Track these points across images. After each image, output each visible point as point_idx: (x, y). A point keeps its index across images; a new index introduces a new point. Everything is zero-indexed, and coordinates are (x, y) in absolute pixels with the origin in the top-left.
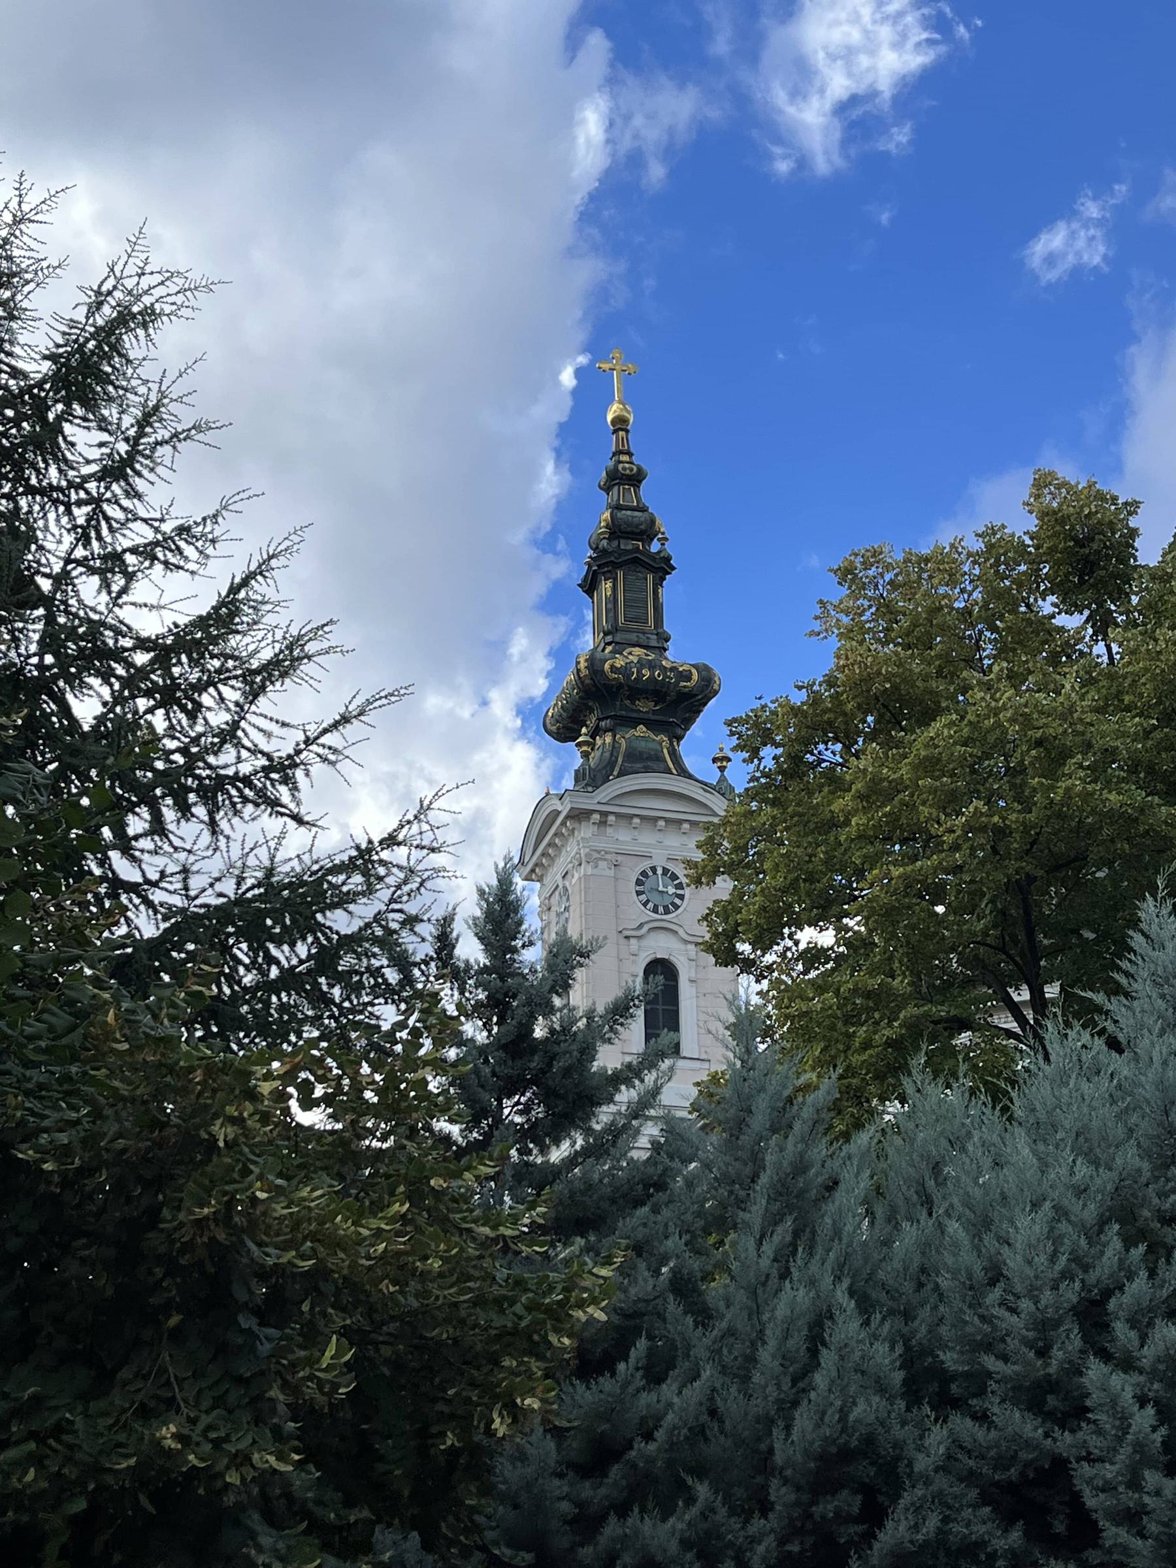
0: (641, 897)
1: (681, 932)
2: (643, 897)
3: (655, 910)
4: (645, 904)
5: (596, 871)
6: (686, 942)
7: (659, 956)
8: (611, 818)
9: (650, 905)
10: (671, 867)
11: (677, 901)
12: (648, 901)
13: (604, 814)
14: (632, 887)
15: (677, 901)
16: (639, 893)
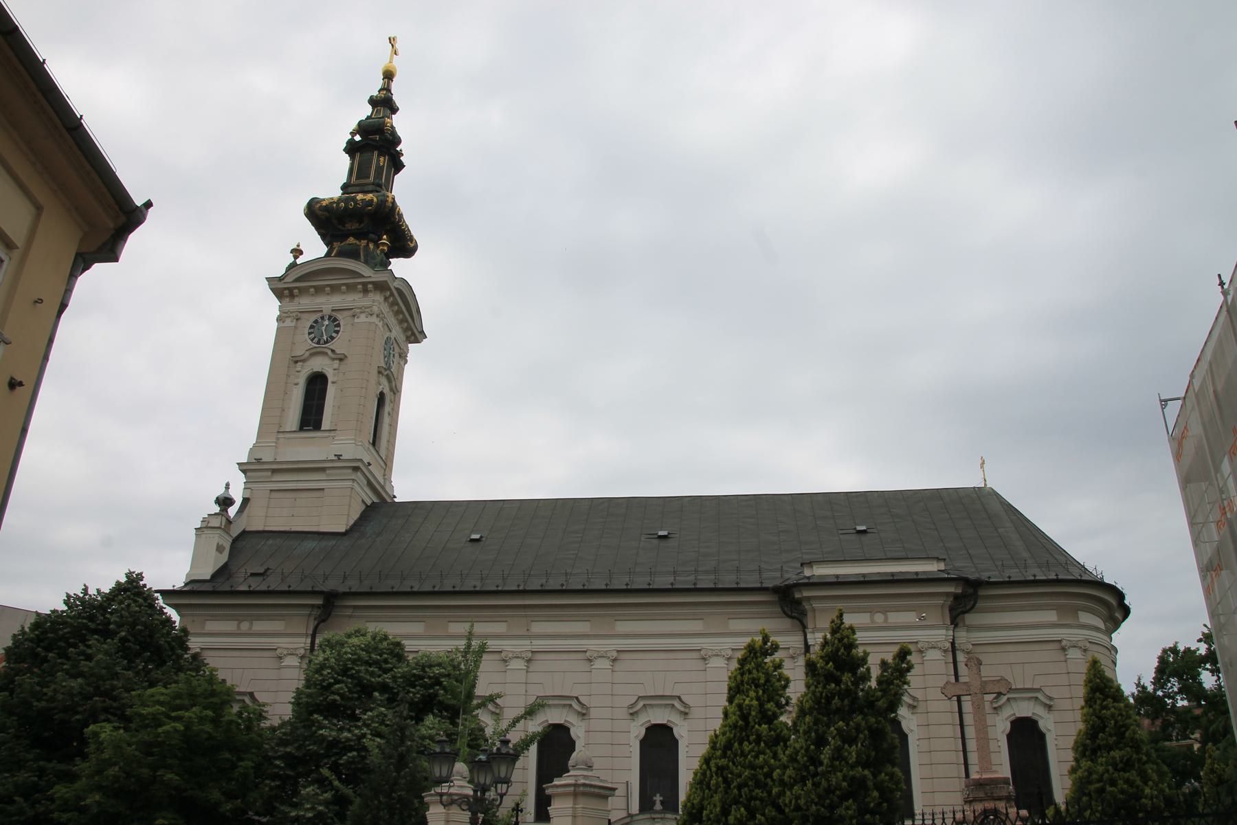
2: (313, 335)
3: (318, 343)
4: (312, 340)
5: (285, 325)
6: (336, 359)
7: (315, 370)
8: (296, 291)
9: (316, 340)
10: (334, 314)
11: (334, 335)
12: (315, 337)
13: (291, 290)
14: (307, 330)
15: (334, 335)
16: (310, 334)
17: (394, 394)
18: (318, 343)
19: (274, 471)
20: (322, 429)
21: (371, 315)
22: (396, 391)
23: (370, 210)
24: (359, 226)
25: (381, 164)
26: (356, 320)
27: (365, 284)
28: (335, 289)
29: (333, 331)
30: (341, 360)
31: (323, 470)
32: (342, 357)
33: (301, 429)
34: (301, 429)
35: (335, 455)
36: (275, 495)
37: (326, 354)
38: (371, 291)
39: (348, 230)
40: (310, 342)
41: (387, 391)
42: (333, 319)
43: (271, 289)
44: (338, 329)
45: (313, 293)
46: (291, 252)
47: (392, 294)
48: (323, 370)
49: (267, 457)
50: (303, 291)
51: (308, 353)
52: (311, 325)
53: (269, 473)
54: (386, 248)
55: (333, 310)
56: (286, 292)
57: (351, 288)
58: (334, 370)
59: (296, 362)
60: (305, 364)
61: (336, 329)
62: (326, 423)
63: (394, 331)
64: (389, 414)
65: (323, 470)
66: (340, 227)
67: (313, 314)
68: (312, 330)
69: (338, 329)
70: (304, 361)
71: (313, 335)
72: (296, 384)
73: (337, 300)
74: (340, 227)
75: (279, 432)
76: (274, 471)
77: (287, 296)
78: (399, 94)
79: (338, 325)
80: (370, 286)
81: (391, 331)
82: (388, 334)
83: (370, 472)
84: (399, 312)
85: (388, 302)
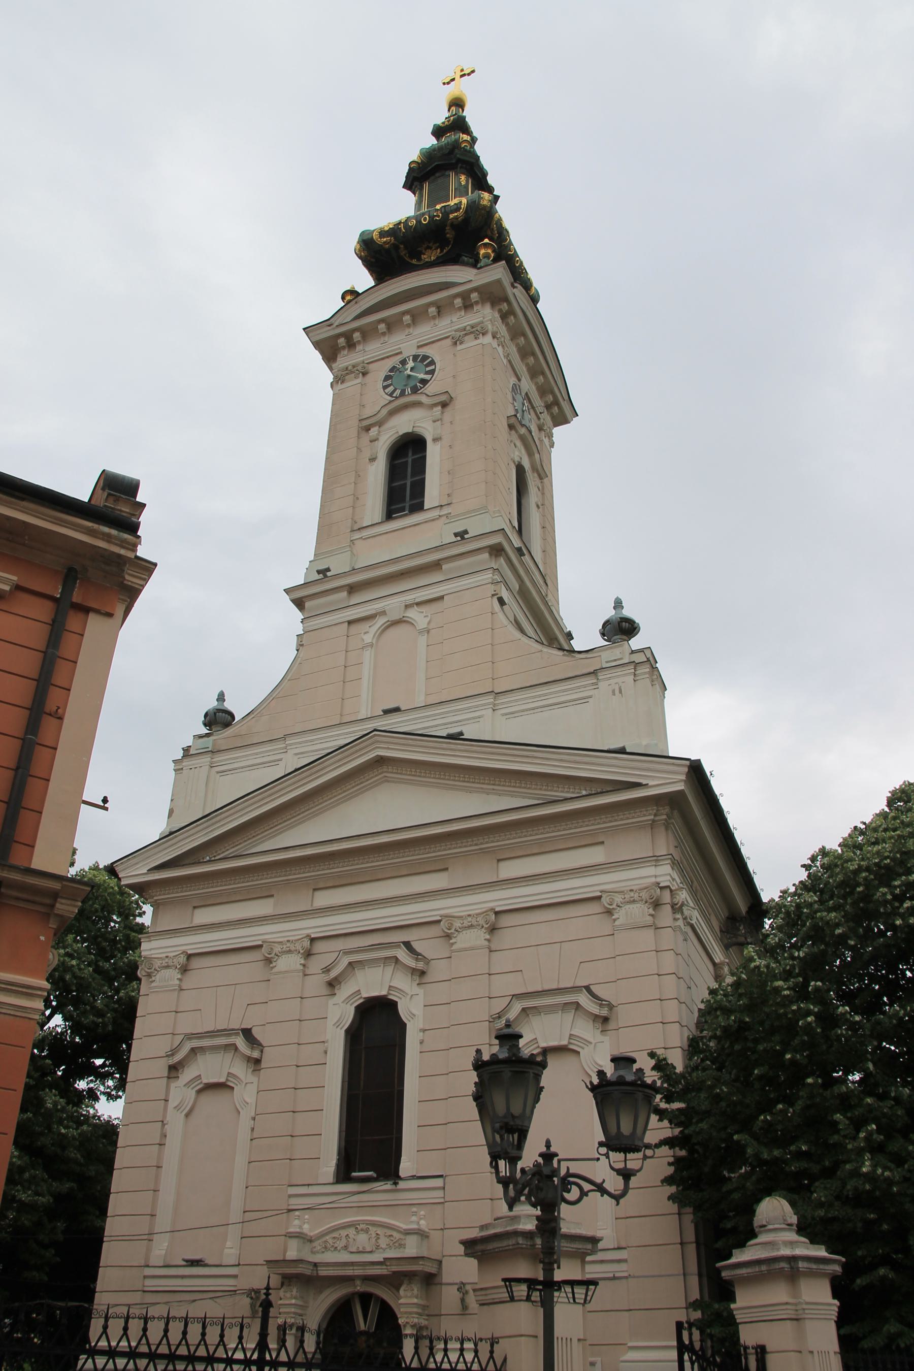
0: (387, 391)
1: (424, 399)
2: (391, 388)
3: (403, 394)
4: (391, 395)
7: (401, 433)
8: (357, 336)
9: (398, 392)
11: (428, 377)
13: (348, 336)
14: (380, 385)
16: (385, 388)
17: (541, 478)
18: (403, 394)
19: (352, 589)
20: (425, 508)
21: (483, 334)
22: (543, 474)
23: (456, 218)
24: (442, 251)
25: (463, 183)
26: (459, 347)
27: (465, 296)
28: (417, 317)
29: (424, 367)
30: (444, 405)
31: (436, 565)
32: (443, 398)
33: (390, 514)
34: (390, 514)
35: (456, 535)
36: (354, 628)
37: (417, 404)
38: (477, 303)
39: (427, 262)
40: (390, 398)
41: (526, 464)
42: (423, 360)
43: (317, 345)
44: (433, 367)
45: (385, 330)
46: (343, 298)
47: (511, 312)
48: (416, 430)
49: (338, 565)
50: (368, 333)
51: (384, 412)
52: (386, 376)
53: (344, 594)
54: (490, 251)
55: (419, 347)
56: (342, 341)
57: (441, 309)
58: (434, 421)
59: (367, 429)
60: (383, 428)
61: (428, 369)
62: (432, 494)
63: (523, 379)
64: (538, 507)
65: (436, 565)
66: (414, 262)
67: (387, 360)
68: (389, 382)
69: (433, 367)
70: (380, 424)
71: (391, 388)
72: (373, 459)
73: (425, 331)
74: (414, 262)
75: (352, 531)
76: (352, 589)
77: (344, 348)
78: (470, 115)
79: (432, 363)
80: (474, 296)
81: (519, 380)
82: (513, 380)
83: (522, 563)
84: (525, 353)
85: (507, 325)
